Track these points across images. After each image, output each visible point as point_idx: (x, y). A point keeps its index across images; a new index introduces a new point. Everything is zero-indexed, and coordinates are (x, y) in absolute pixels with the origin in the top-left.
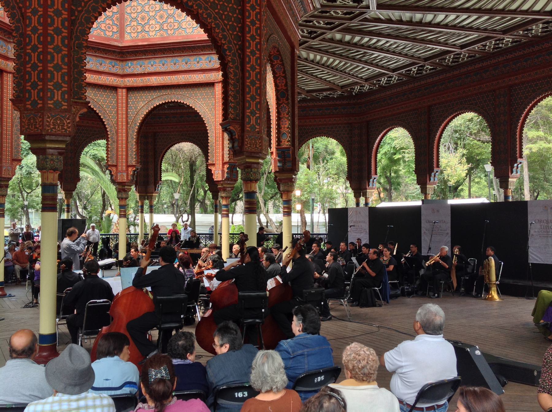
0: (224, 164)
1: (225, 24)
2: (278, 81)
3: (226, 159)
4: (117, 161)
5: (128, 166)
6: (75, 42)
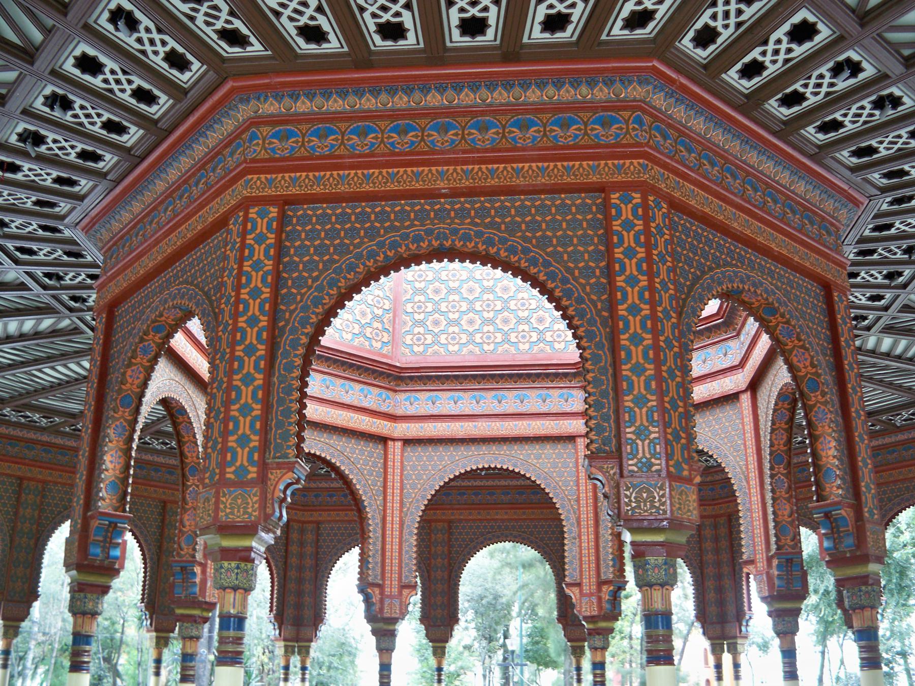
0: (769, 560)
1: (568, 270)
2: (795, 360)
3: (774, 547)
4: (581, 578)
5: (601, 584)
6: (281, 361)
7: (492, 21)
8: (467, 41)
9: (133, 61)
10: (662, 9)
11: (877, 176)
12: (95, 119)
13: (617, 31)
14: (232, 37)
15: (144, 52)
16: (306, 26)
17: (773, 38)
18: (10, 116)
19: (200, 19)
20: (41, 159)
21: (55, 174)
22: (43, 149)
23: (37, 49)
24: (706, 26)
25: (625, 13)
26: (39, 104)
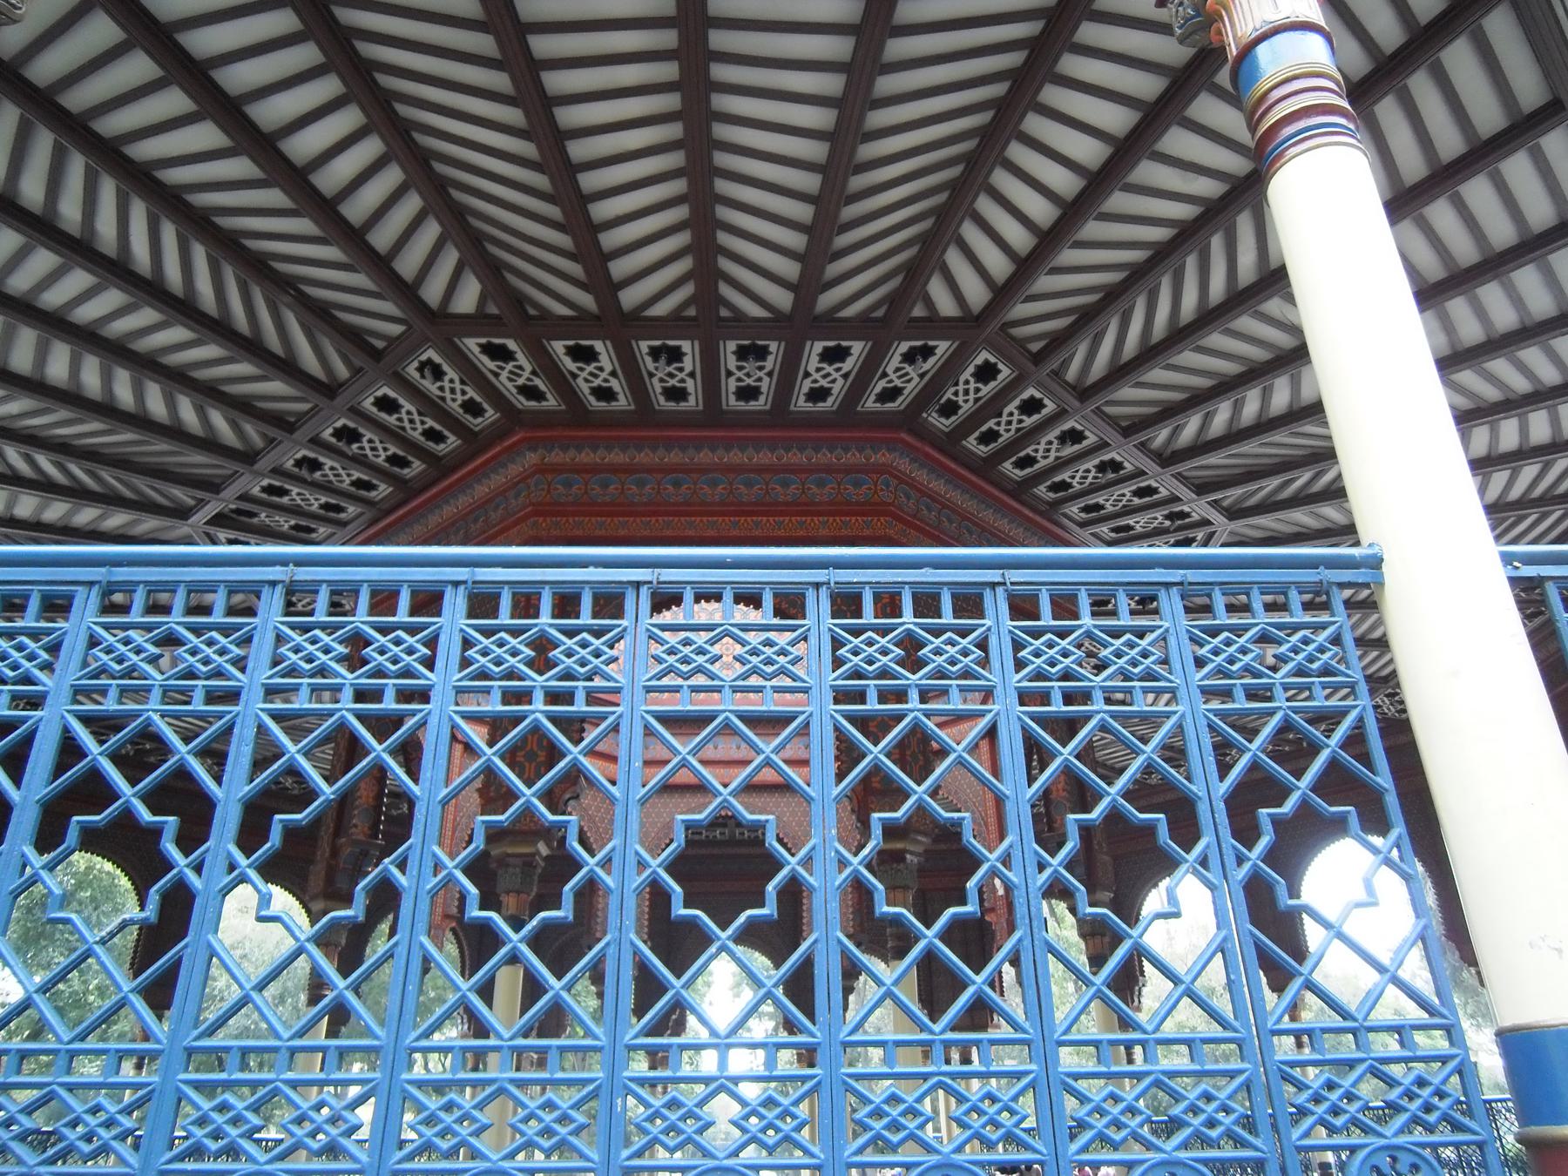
7: (764, 389)
8: (741, 406)
9: (430, 405)
10: (910, 386)
11: (1105, 529)
12: (379, 450)
13: (870, 404)
14: (530, 392)
15: (443, 399)
16: (600, 387)
17: (1006, 411)
18: (296, 443)
19: (504, 375)
20: (315, 485)
21: (323, 500)
22: (318, 474)
23: (341, 385)
24: (949, 400)
25: (878, 389)
26: (327, 434)
